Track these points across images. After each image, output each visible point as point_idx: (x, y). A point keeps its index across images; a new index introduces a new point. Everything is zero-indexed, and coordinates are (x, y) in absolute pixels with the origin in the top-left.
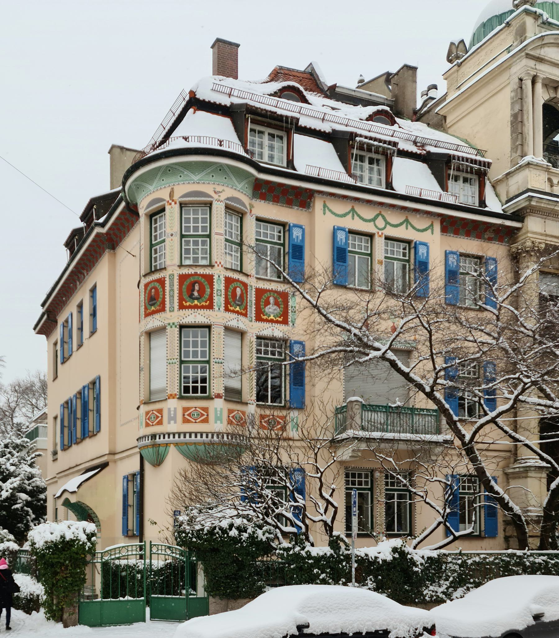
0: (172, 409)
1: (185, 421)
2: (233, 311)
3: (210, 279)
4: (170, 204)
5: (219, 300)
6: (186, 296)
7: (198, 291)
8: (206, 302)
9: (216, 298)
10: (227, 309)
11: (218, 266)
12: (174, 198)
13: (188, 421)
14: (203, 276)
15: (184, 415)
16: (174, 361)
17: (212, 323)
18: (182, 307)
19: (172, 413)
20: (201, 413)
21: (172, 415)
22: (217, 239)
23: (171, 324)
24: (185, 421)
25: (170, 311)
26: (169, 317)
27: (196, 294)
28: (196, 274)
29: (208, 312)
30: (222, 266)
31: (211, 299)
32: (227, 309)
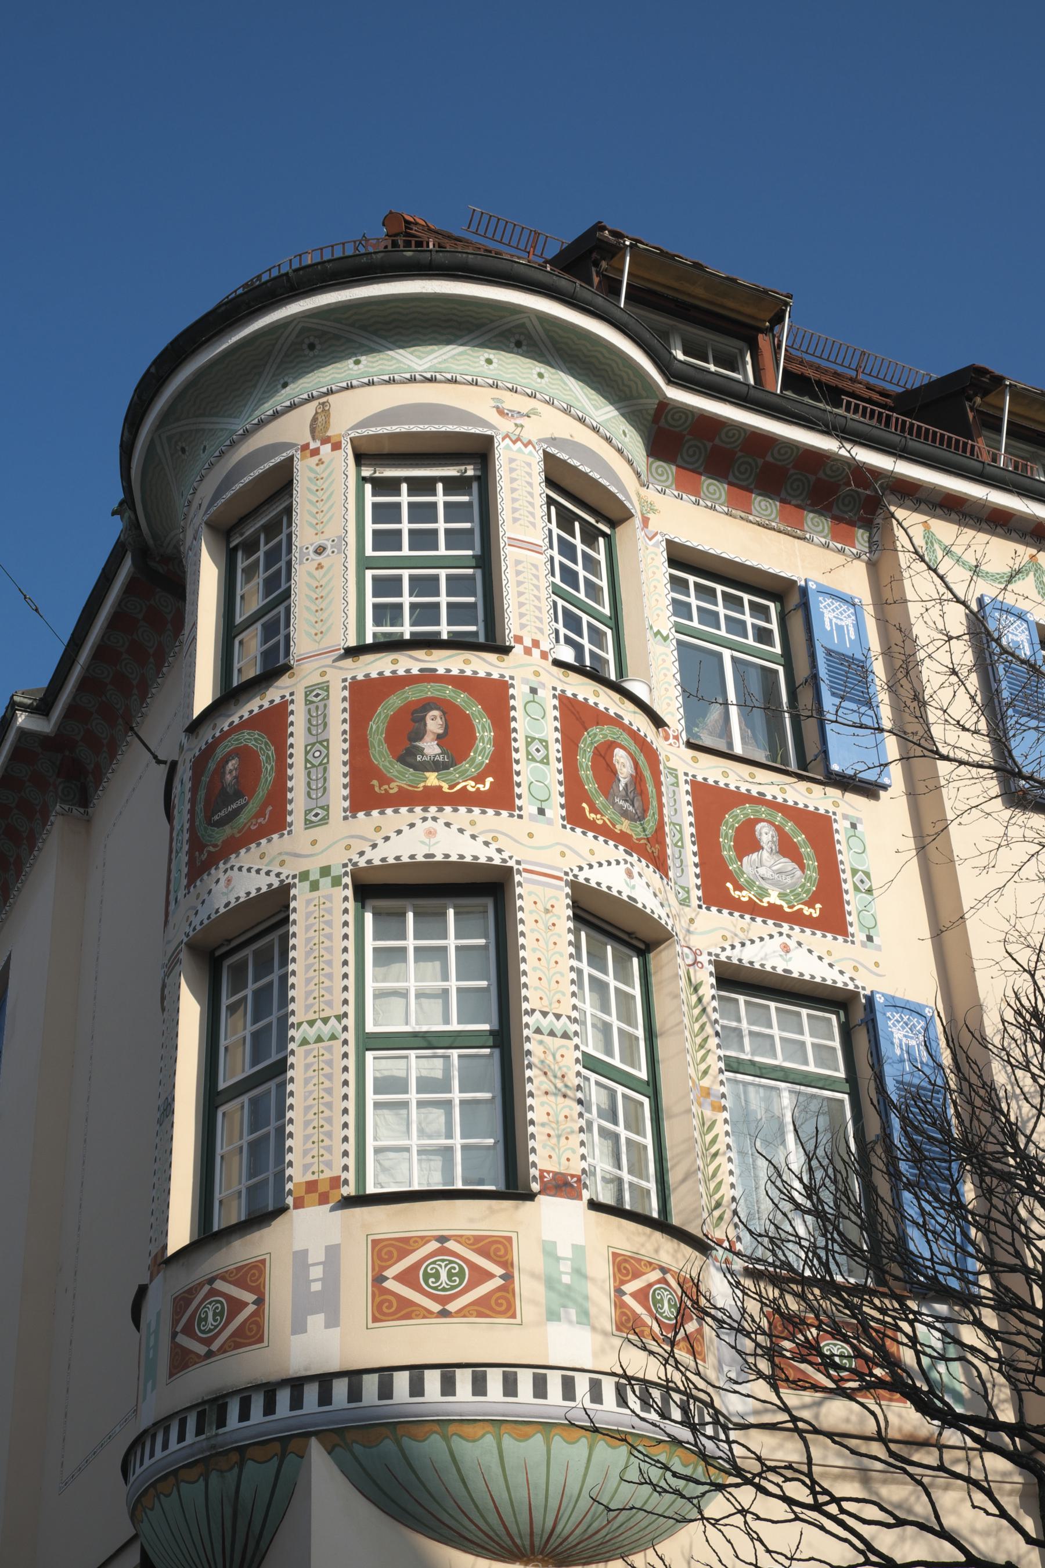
0: (317, 1255)
2: (605, 832)
3: (495, 696)
4: (316, 452)
5: (539, 777)
7: (439, 737)
9: (525, 771)
10: (575, 818)
11: (528, 651)
13: (405, 1310)
14: (461, 682)
15: (379, 1279)
16: (326, 1030)
17: (511, 863)
19: (316, 1272)
21: (316, 1287)
22: (518, 562)
24: (387, 1308)
25: (309, 824)
26: (308, 849)
27: (430, 748)
28: (428, 676)
29: (488, 820)
30: (544, 655)
31: (501, 766)
32: (575, 818)
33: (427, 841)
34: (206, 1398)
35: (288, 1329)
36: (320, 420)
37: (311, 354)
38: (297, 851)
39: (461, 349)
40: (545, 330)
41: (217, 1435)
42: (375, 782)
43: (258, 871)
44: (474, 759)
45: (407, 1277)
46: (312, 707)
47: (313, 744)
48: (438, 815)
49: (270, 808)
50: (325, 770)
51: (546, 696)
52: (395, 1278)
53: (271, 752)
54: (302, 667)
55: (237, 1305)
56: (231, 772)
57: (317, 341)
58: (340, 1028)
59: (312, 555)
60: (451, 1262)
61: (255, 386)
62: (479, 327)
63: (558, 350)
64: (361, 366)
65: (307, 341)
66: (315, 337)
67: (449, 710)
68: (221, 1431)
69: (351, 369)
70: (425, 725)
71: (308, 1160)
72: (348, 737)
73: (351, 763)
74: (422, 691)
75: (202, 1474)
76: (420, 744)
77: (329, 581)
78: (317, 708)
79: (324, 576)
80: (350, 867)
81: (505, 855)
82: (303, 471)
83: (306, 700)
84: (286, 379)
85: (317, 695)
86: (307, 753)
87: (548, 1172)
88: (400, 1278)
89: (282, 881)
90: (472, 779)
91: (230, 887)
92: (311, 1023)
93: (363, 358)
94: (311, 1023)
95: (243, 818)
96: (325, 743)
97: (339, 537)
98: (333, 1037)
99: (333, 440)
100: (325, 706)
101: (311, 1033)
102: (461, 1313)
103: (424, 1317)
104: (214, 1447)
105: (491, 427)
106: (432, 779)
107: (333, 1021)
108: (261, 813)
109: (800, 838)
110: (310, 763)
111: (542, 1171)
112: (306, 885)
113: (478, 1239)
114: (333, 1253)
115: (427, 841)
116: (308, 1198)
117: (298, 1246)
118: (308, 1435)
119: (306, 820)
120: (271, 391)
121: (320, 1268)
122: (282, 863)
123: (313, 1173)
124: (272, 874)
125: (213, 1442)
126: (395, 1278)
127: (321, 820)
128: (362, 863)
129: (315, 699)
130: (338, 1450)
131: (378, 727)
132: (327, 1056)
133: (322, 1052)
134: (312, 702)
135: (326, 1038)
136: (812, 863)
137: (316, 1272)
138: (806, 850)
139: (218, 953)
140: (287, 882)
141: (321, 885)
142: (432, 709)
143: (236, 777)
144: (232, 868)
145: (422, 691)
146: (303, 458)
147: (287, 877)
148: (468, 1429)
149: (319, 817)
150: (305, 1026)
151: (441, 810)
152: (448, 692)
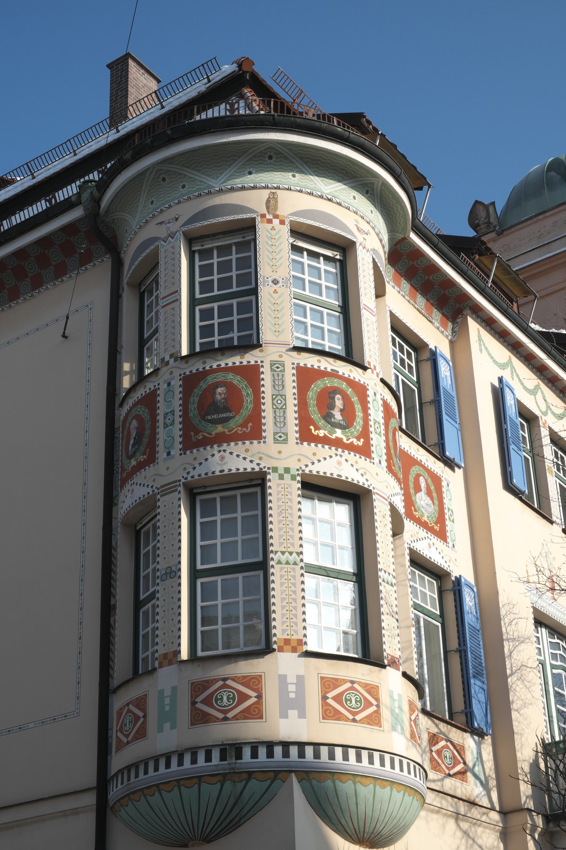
0: (291, 679)
1: (329, 714)
6: (315, 415)
7: (341, 411)
8: (358, 439)
12: (278, 213)
13: (337, 716)
14: (350, 382)
15: (324, 698)
16: (291, 559)
17: (371, 488)
18: (306, 436)
19: (292, 688)
20: (366, 699)
21: (292, 695)
23: (281, 471)
24: (329, 714)
25: (276, 441)
26: (277, 455)
27: (338, 416)
28: (334, 374)
33: (338, 467)
34: (225, 742)
35: (278, 715)
36: (272, 202)
37: (269, 161)
38: (270, 454)
39: (344, 186)
40: (381, 188)
41: (236, 763)
42: (312, 427)
43: (244, 459)
44: (356, 427)
45: (337, 698)
46: (275, 374)
47: (277, 396)
48: (342, 454)
49: (250, 424)
50: (284, 412)
51: (378, 397)
52: (332, 698)
53: (250, 391)
54: (268, 348)
55: (244, 697)
56: (220, 394)
57: (274, 156)
58: (299, 559)
59: (271, 284)
60: (357, 695)
61: (230, 166)
62: (354, 177)
63: (381, 200)
64: (295, 179)
65: (269, 154)
66: (274, 153)
67: (346, 398)
68: (239, 761)
69: (289, 178)
70: (335, 402)
71: (284, 627)
72: (296, 397)
73: (299, 412)
74: (332, 382)
75: (220, 781)
76: (333, 412)
77: (282, 302)
78: (278, 375)
79: (278, 298)
80: (300, 472)
81: (369, 483)
82: (262, 228)
83: (271, 369)
84: (251, 170)
85: (278, 368)
86: (273, 399)
87: (390, 655)
88: (334, 698)
89: (261, 469)
90: (355, 438)
91: (224, 462)
92: (283, 553)
93: (297, 175)
94: (283, 553)
95: (232, 424)
96: (284, 397)
97: (286, 278)
98: (295, 563)
99: (280, 218)
100: (283, 375)
101: (283, 558)
102: (361, 721)
103: (346, 721)
104: (233, 769)
105: (355, 237)
106: (339, 433)
107: (294, 555)
108: (244, 425)
109: (432, 488)
110: (276, 406)
111: (388, 654)
112: (276, 475)
113: (367, 685)
114: (300, 680)
115: (338, 467)
116: (286, 647)
117: (281, 672)
118: (291, 772)
119: (274, 438)
120: (240, 173)
121: (294, 686)
122: (261, 459)
123: (288, 635)
124: (255, 463)
125: (233, 766)
126: (332, 698)
127: (283, 440)
128: (307, 471)
129: (276, 369)
130: (304, 781)
131: (312, 396)
132: (292, 573)
133: (289, 570)
134: (275, 371)
135: (291, 563)
136: (436, 502)
137: (292, 688)
138: (435, 495)
139: (195, 491)
140: (264, 470)
141: (285, 477)
142: (337, 394)
143: (224, 399)
144: (225, 451)
145: (332, 382)
146: (262, 222)
147: (265, 467)
148: (364, 780)
149: (282, 438)
150: (279, 554)
151: (343, 452)
152: (344, 386)
